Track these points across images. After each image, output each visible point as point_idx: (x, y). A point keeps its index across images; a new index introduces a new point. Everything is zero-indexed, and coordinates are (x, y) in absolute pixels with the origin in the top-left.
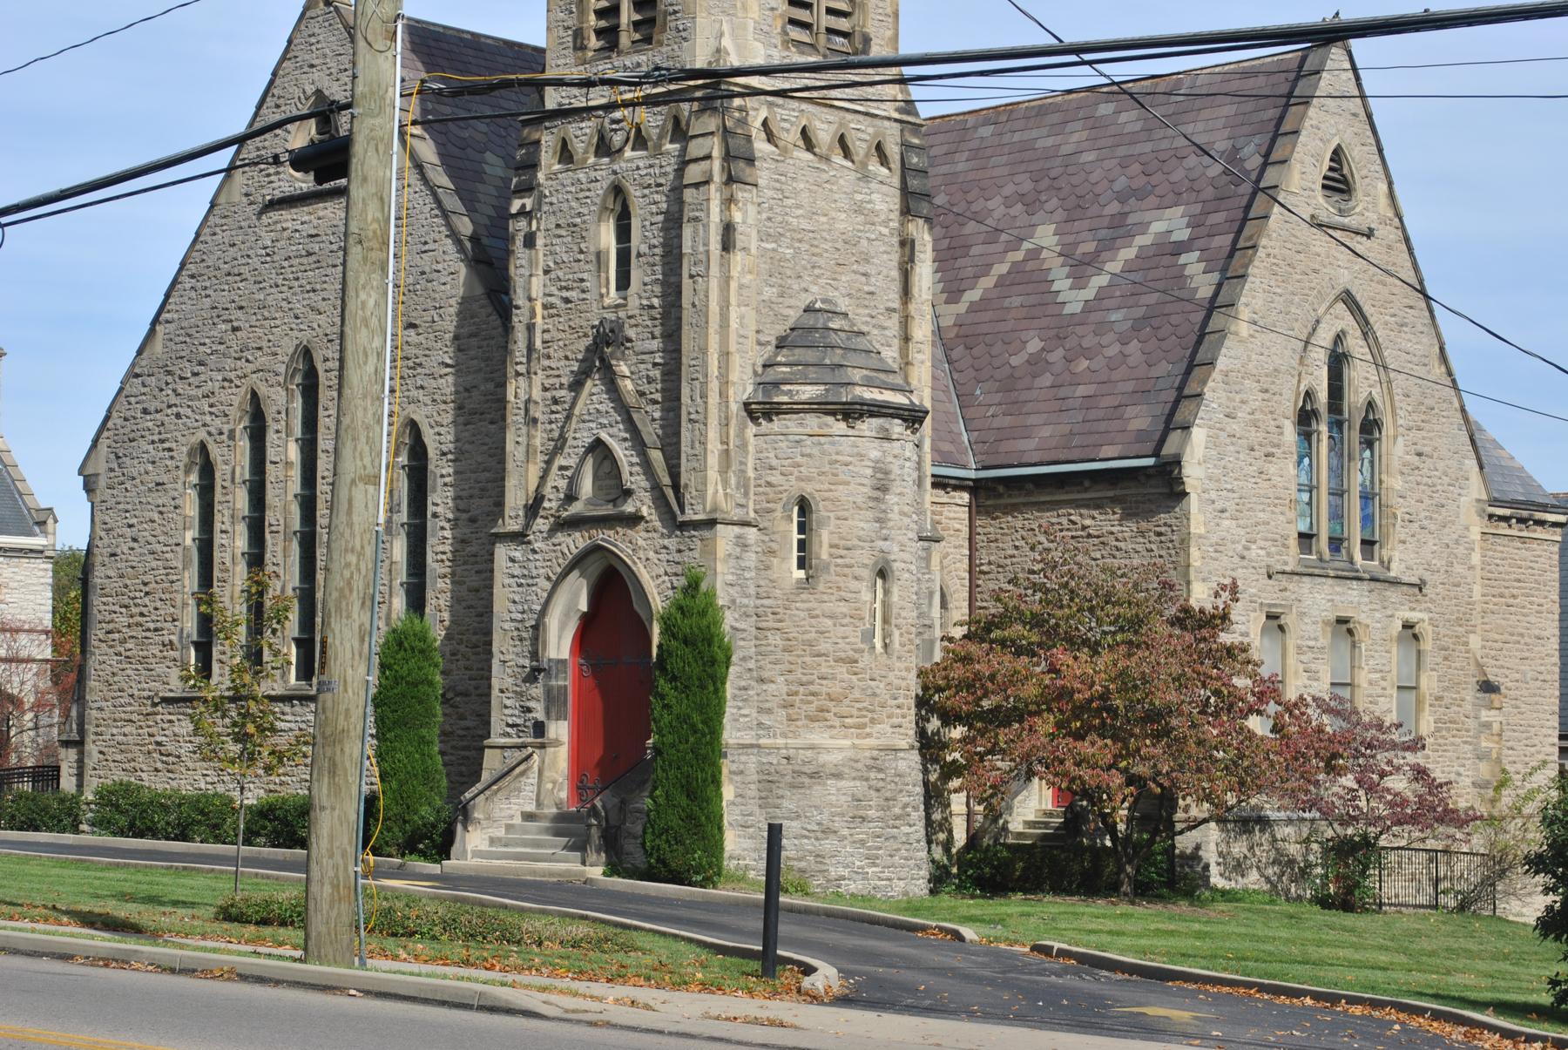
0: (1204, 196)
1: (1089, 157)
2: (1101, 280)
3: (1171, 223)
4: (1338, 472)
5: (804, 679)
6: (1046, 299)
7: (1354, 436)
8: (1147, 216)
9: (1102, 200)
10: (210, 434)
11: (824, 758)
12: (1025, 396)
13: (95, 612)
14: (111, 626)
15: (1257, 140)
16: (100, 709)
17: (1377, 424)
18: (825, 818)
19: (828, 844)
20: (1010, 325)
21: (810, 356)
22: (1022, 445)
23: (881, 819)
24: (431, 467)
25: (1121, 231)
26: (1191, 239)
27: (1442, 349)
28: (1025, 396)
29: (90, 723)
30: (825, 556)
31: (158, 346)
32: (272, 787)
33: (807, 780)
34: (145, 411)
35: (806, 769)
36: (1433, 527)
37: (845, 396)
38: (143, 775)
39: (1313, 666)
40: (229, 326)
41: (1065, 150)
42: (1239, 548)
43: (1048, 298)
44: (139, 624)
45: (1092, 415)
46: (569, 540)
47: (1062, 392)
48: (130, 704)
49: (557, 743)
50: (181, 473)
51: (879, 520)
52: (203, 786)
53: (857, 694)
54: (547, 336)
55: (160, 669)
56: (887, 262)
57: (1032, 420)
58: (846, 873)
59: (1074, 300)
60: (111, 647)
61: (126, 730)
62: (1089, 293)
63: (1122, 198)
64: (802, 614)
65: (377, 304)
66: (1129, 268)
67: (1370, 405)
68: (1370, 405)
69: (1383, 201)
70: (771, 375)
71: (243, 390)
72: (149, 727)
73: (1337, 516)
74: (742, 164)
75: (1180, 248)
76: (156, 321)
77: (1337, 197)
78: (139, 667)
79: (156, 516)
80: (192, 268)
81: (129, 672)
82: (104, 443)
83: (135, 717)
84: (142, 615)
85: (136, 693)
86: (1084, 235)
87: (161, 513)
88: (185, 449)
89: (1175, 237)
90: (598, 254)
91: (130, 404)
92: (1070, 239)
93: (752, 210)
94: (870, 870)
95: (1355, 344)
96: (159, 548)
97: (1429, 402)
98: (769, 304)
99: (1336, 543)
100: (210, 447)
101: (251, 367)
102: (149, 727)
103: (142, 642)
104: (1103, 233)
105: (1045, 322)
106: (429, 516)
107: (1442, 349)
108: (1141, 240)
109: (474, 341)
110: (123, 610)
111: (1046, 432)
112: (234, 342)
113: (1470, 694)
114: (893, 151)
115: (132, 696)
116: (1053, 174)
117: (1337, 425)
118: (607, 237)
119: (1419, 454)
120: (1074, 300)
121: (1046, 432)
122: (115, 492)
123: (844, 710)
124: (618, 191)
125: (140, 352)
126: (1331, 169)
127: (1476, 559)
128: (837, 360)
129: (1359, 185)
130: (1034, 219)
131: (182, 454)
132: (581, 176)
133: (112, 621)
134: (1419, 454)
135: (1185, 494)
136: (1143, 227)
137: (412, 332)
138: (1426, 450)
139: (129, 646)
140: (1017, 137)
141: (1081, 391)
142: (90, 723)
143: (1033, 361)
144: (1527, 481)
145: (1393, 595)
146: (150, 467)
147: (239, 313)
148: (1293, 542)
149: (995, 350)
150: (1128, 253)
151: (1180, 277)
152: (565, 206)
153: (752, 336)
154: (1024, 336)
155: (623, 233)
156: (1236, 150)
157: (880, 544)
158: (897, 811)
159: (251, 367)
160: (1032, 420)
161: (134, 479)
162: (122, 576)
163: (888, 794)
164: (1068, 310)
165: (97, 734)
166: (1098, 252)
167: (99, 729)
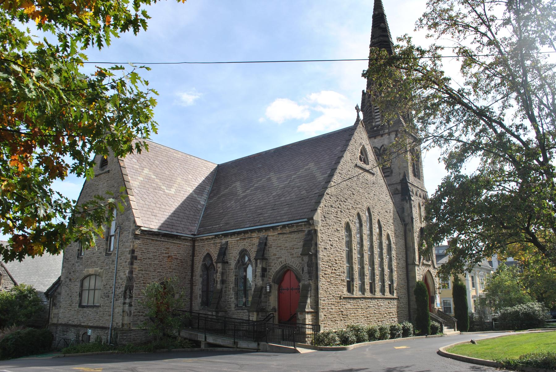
10: (350, 220)
13: (321, 267)
16: (324, 300)
29: (321, 305)
44: (334, 273)
79: (337, 240)
84: (335, 270)
87: (339, 239)
91: (326, 202)
96: (339, 250)
100: (351, 224)
103: (336, 279)
115: (334, 296)
142: (321, 305)
161: (330, 226)
165: (323, 309)
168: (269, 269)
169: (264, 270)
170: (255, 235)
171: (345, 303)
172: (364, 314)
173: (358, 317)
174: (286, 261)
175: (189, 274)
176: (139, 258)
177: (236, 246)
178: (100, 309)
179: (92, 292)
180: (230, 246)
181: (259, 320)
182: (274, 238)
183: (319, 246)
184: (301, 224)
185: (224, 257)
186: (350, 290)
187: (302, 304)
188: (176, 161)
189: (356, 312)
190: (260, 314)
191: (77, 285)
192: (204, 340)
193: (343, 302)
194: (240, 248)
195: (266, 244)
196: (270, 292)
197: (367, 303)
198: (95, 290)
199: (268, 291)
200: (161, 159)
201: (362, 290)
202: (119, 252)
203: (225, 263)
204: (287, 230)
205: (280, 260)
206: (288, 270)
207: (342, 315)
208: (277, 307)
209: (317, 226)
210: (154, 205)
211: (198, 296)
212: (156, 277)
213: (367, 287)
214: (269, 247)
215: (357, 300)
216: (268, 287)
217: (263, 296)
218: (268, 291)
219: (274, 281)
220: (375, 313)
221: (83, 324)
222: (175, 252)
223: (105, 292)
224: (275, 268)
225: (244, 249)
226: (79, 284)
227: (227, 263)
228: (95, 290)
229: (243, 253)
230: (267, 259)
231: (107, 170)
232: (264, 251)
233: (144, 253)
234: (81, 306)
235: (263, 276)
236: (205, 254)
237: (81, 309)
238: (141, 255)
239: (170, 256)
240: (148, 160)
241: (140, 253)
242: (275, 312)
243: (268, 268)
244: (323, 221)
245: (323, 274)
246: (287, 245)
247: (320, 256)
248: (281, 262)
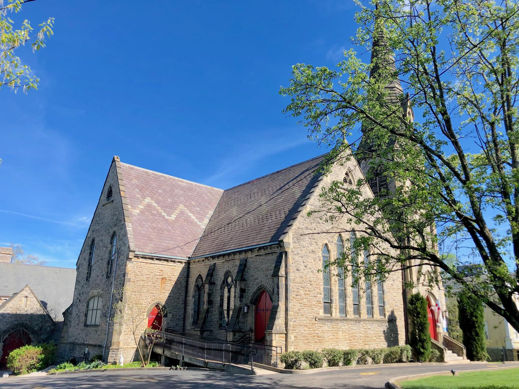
13: (291, 288)
14: (298, 293)
32: (352, 346)
38: (312, 344)
44: (308, 294)
48: (306, 320)
55: (316, 309)
60: (298, 300)
72: (313, 328)
78: (309, 308)
79: (313, 261)
81: (305, 310)
84: (309, 291)
85: (308, 317)
102: (313, 328)
110: (302, 289)
122: (297, 250)
133: (299, 292)
139: (304, 301)
142: (290, 327)
167: (294, 329)
168: (248, 290)
169: (243, 291)
170: (237, 256)
171: (320, 325)
172: (346, 337)
174: (261, 282)
175: (182, 294)
176: (132, 281)
177: (222, 268)
178: (99, 328)
179: (95, 312)
180: (218, 267)
181: (236, 340)
182: (253, 260)
183: (290, 268)
184: (274, 246)
185: (211, 278)
187: (270, 325)
188: (180, 189)
189: (335, 334)
190: (237, 334)
191: (84, 306)
192: (182, 359)
193: (318, 324)
194: (225, 270)
195: (245, 266)
196: (248, 312)
197: (350, 326)
198: (97, 310)
199: (246, 311)
200: (165, 188)
201: (344, 310)
202: (116, 275)
203: (212, 283)
204: (262, 252)
205: (257, 281)
206: (264, 291)
207: (318, 337)
208: (253, 328)
209: (288, 248)
210: (152, 231)
211: (191, 316)
212: (149, 298)
213: (350, 309)
214: (248, 269)
215: (336, 322)
216: (246, 307)
217: (241, 316)
218: (246, 311)
219: (251, 302)
220: (360, 336)
221: (85, 343)
222: (169, 274)
223: (104, 312)
224: (252, 289)
225: (228, 270)
226: (85, 305)
227: (214, 283)
228: (97, 310)
229: (227, 274)
230: (245, 280)
231: (112, 200)
232: (243, 272)
233: (138, 275)
234: (86, 325)
235: (241, 297)
236: (197, 276)
237: (86, 328)
238: (135, 277)
239: (164, 278)
240: (152, 189)
241: (133, 276)
242: (252, 332)
243: (247, 289)
244: (296, 243)
245: (294, 296)
246: (262, 266)
247: (291, 277)
248: (258, 283)
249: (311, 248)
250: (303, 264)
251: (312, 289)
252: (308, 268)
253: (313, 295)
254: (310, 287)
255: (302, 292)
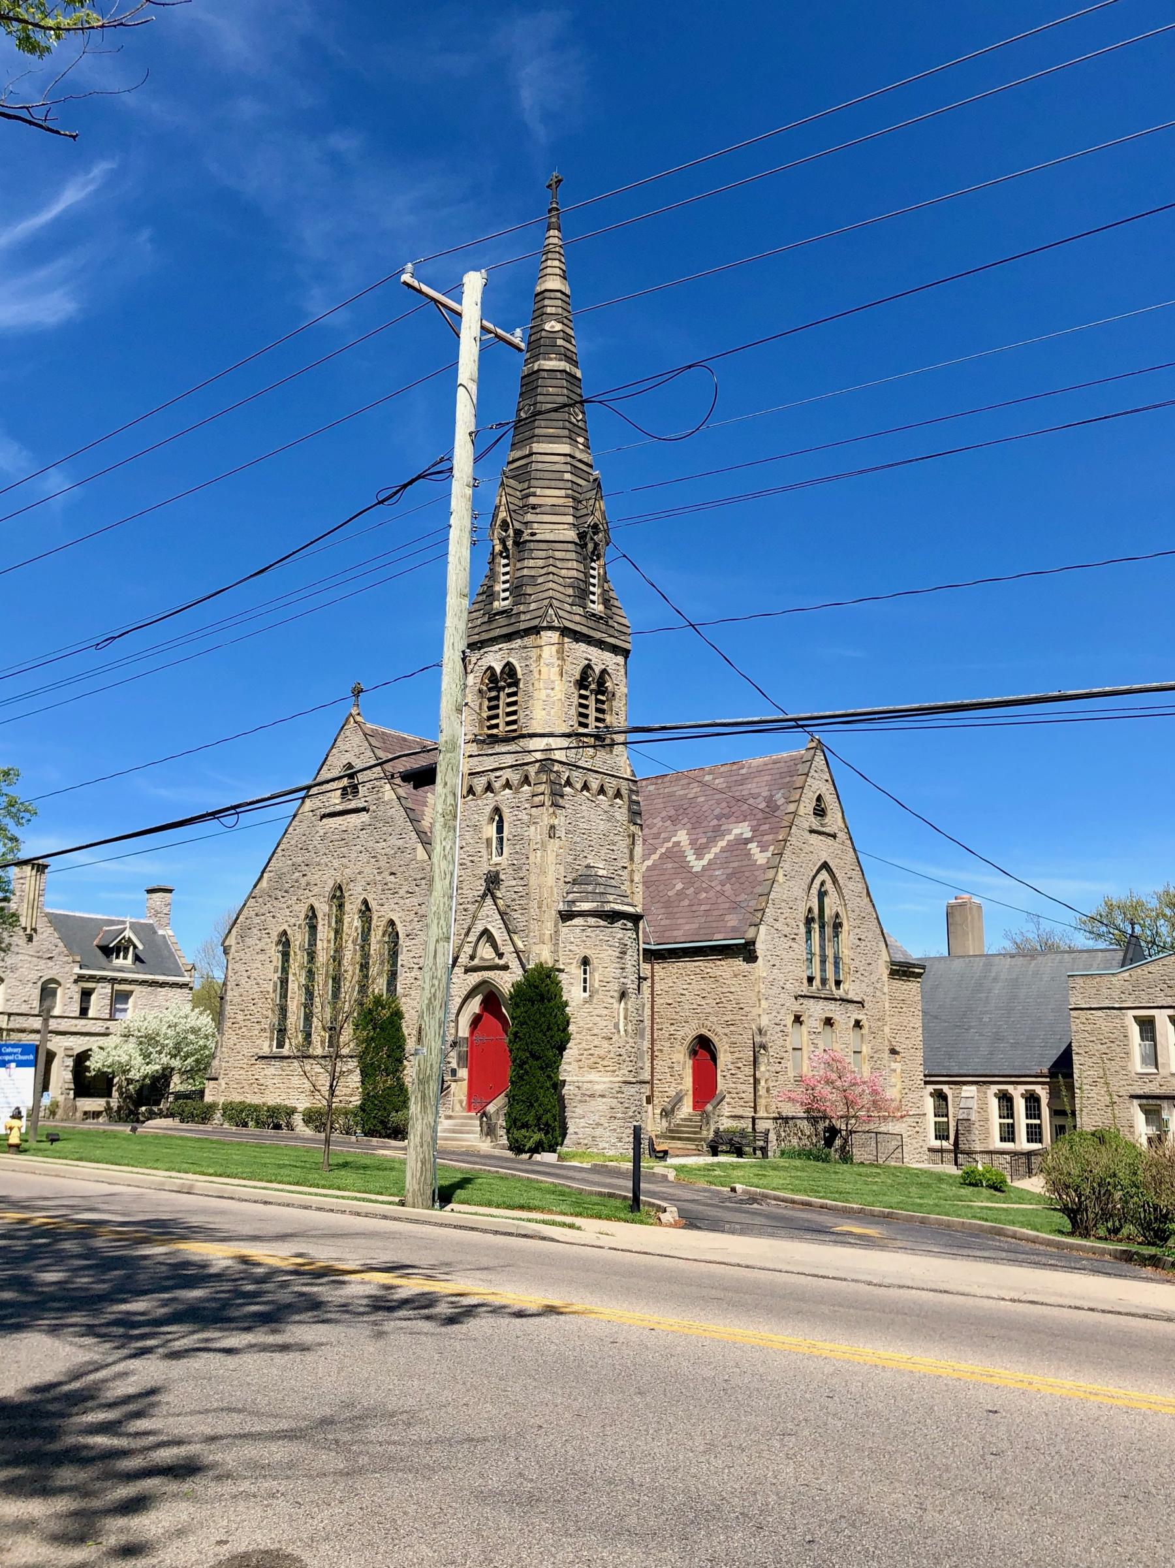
0: (757, 817)
1: (702, 799)
2: (709, 856)
3: (743, 829)
4: (822, 948)
5: (587, 1047)
6: (684, 867)
7: (828, 930)
8: (731, 826)
9: (709, 819)
11: (597, 1087)
12: (675, 910)
15: (782, 791)
17: (840, 925)
18: (596, 1118)
19: (599, 1131)
20: (667, 877)
21: (590, 888)
22: (675, 933)
23: (624, 1118)
24: (401, 942)
25: (719, 833)
26: (753, 837)
27: (868, 890)
28: (675, 910)
30: (596, 986)
31: (264, 883)
33: (588, 1098)
34: (257, 915)
35: (587, 1093)
36: (866, 974)
37: (607, 907)
39: (815, 1041)
40: (301, 874)
41: (690, 796)
42: (781, 983)
43: (684, 864)
45: (709, 919)
46: (471, 978)
47: (694, 908)
49: (463, 1080)
50: (274, 945)
51: (622, 969)
52: (278, 1101)
53: (612, 1055)
54: (461, 879)
55: (258, 1042)
56: (623, 844)
57: (679, 921)
58: (607, 1145)
59: (697, 865)
61: (240, 1073)
62: (705, 862)
63: (718, 818)
64: (586, 1015)
65: (451, 848)
66: (723, 850)
67: (837, 916)
68: (837, 916)
69: (840, 820)
70: (571, 897)
71: (307, 905)
73: (823, 970)
74: (558, 797)
75: (747, 841)
76: (263, 872)
77: (819, 818)
79: (259, 966)
80: (282, 846)
82: (234, 931)
83: (245, 1066)
86: (699, 836)
88: (276, 934)
89: (744, 836)
90: (487, 840)
92: (694, 837)
93: (563, 818)
94: (619, 1144)
95: (829, 886)
97: (863, 915)
98: (569, 864)
99: (824, 981)
101: (311, 894)
104: (709, 834)
105: (684, 875)
106: (399, 966)
107: (868, 890)
108: (728, 837)
109: (423, 882)
111: (687, 927)
112: (303, 881)
113: (886, 1054)
114: (624, 792)
116: (685, 807)
117: (822, 927)
118: (491, 831)
119: (860, 939)
120: (697, 865)
121: (687, 927)
123: (605, 1063)
124: (497, 810)
125: (255, 886)
126: (817, 805)
127: (886, 990)
128: (602, 891)
129: (829, 812)
130: (676, 828)
131: (275, 937)
132: (479, 802)
134: (860, 939)
135: (757, 957)
136: (729, 832)
137: (392, 877)
138: (862, 937)
140: (667, 790)
141: (703, 908)
143: (680, 893)
144: (904, 953)
145: (851, 1007)
146: (258, 942)
147: (306, 868)
148: (805, 981)
149: (661, 888)
150: (723, 843)
151: (748, 854)
152: (472, 817)
153: (562, 879)
154: (674, 882)
155: (500, 830)
156: (772, 796)
157: (622, 980)
158: (631, 1114)
159: (311, 894)
160: (679, 921)
162: (241, 996)
163: (627, 1105)
164: (694, 870)
166: (707, 842)
173: (289, 1090)
186: (280, 1045)
193: (260, 1064)
215: (289, 1060)
245: (229, 1024)
249: (261, 945)
250: (246, 974)
251: (255, 1011)
252: (252, 978)
253: (256, 1020)
254: (253, 1007)
255: (240, 1017)
